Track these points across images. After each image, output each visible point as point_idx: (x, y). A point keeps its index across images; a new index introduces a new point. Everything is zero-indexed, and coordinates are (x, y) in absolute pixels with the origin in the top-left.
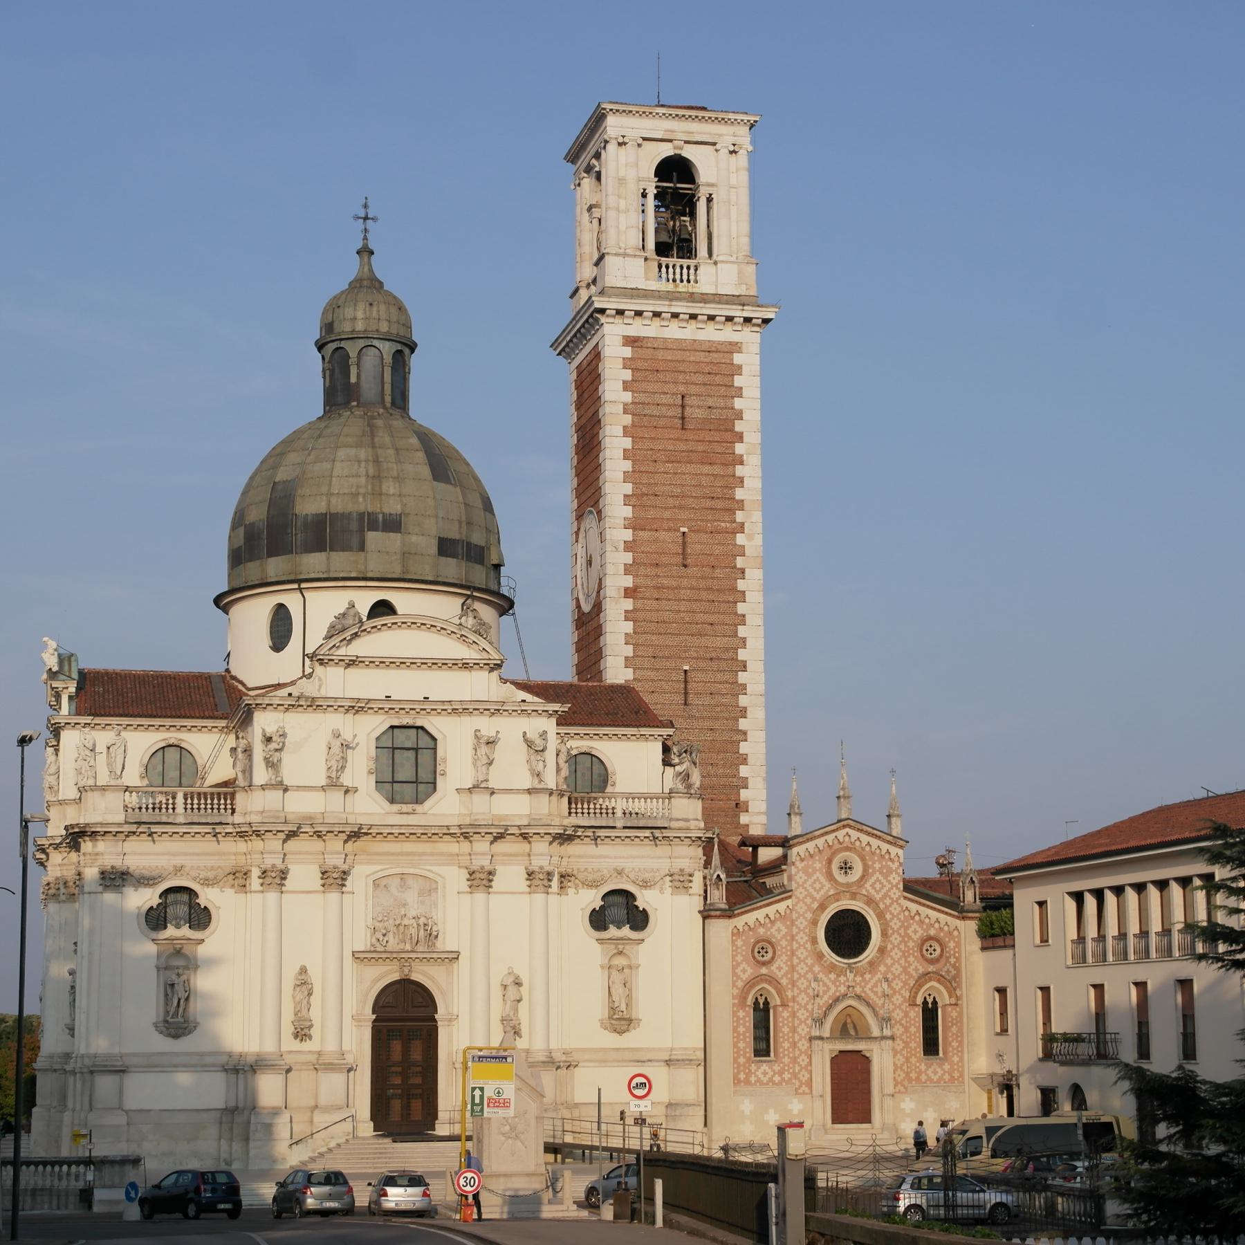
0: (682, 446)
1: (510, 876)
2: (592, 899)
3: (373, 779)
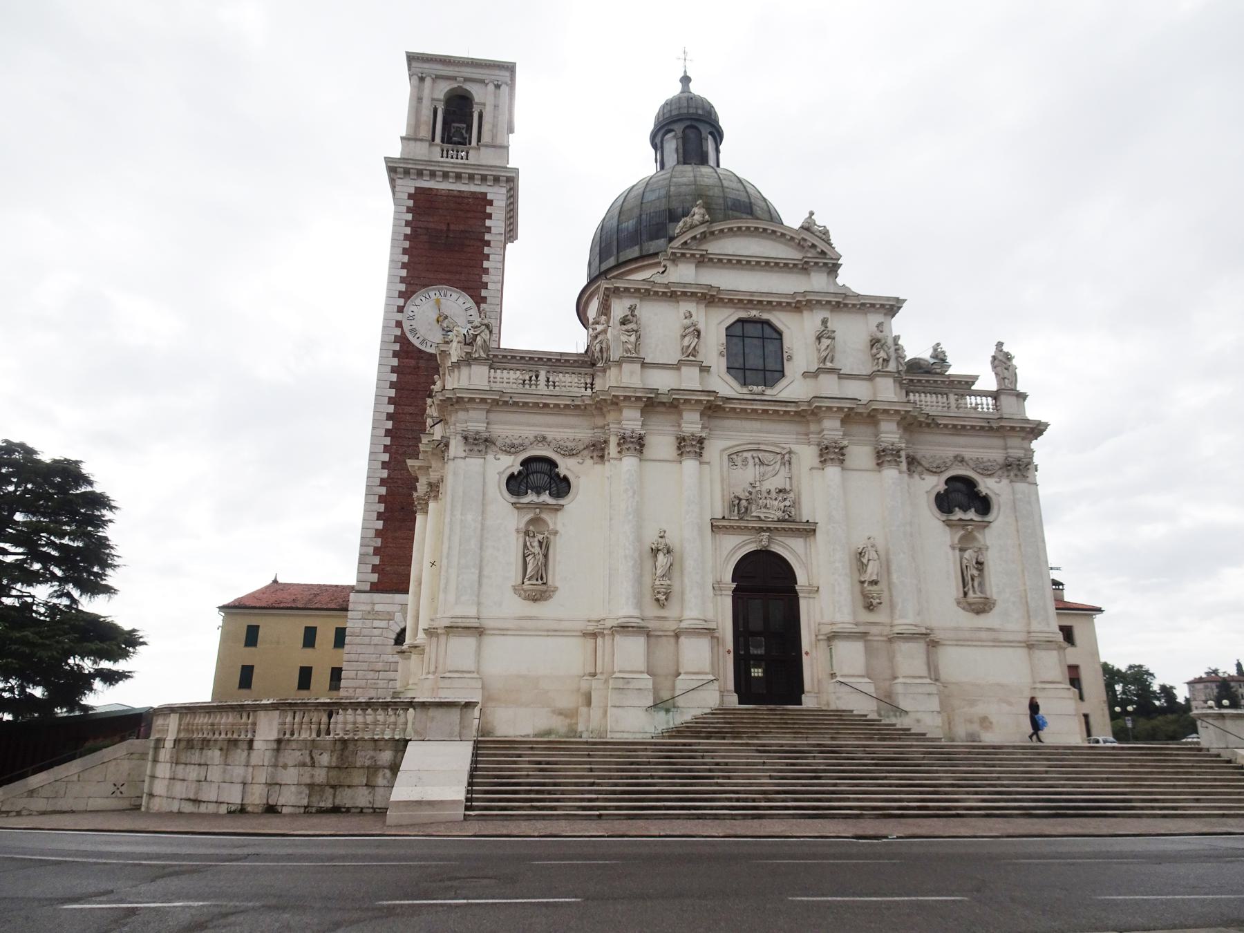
1: (861, 454)
2: (936, 483)
3: (723, 363)
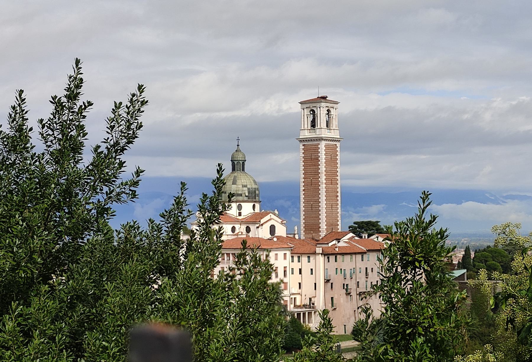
0: (311, 163)
